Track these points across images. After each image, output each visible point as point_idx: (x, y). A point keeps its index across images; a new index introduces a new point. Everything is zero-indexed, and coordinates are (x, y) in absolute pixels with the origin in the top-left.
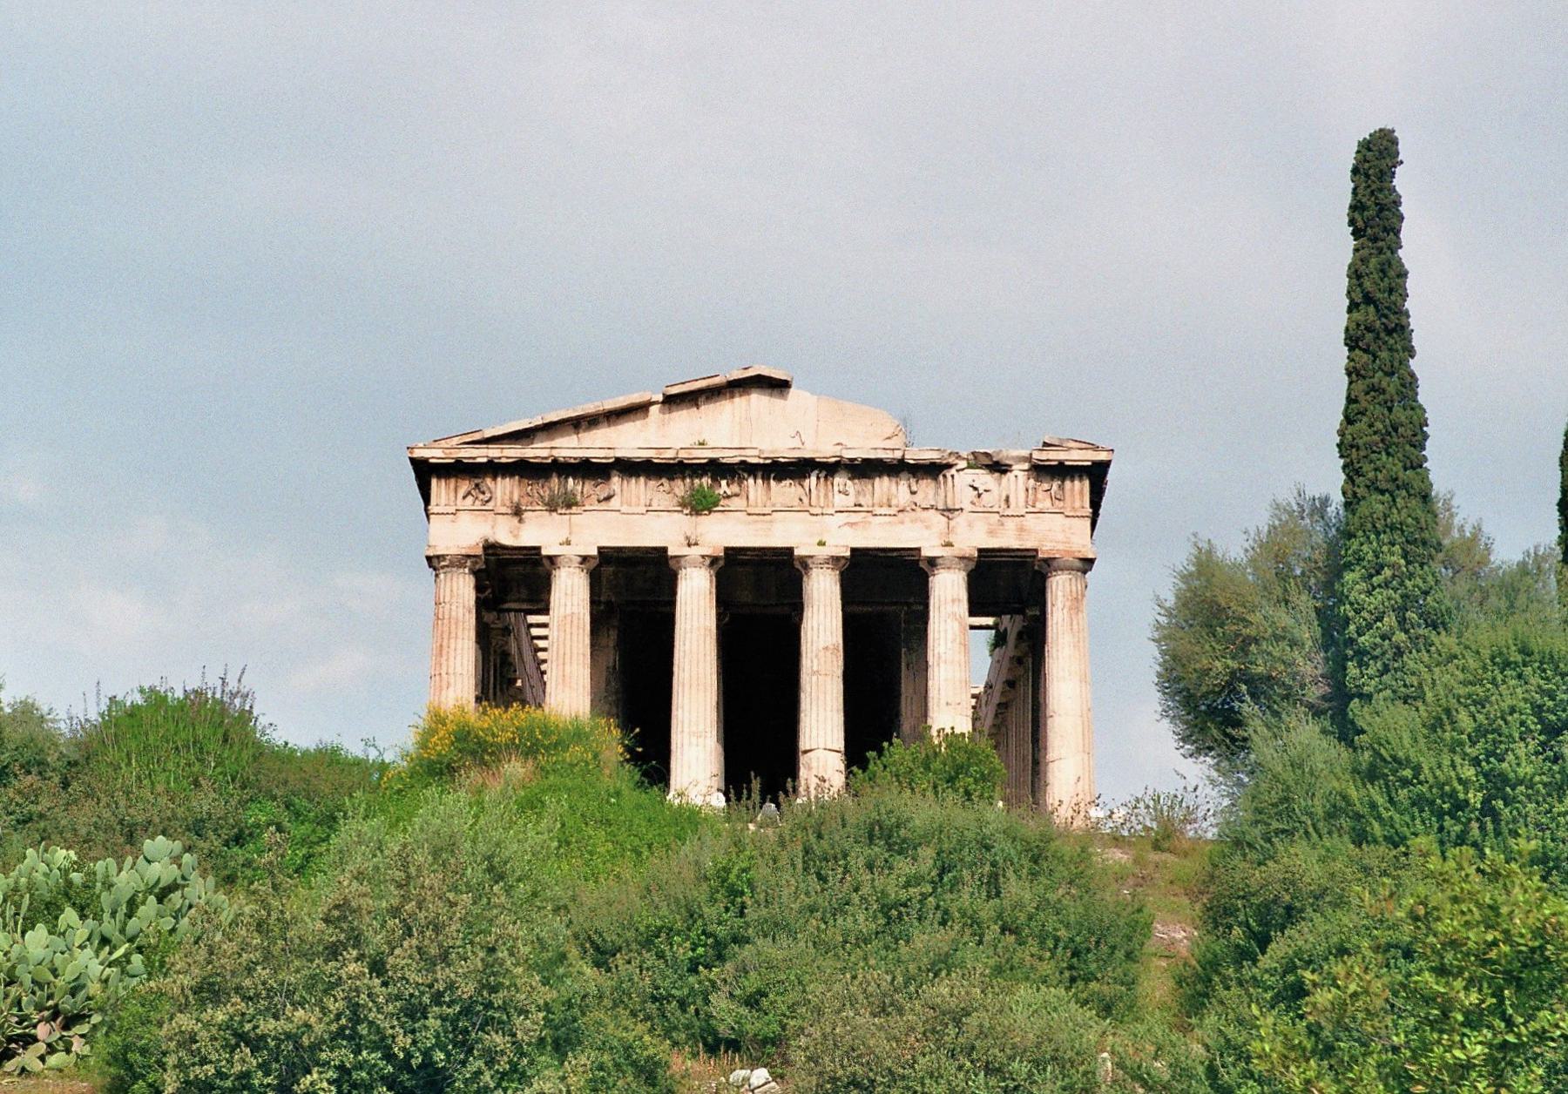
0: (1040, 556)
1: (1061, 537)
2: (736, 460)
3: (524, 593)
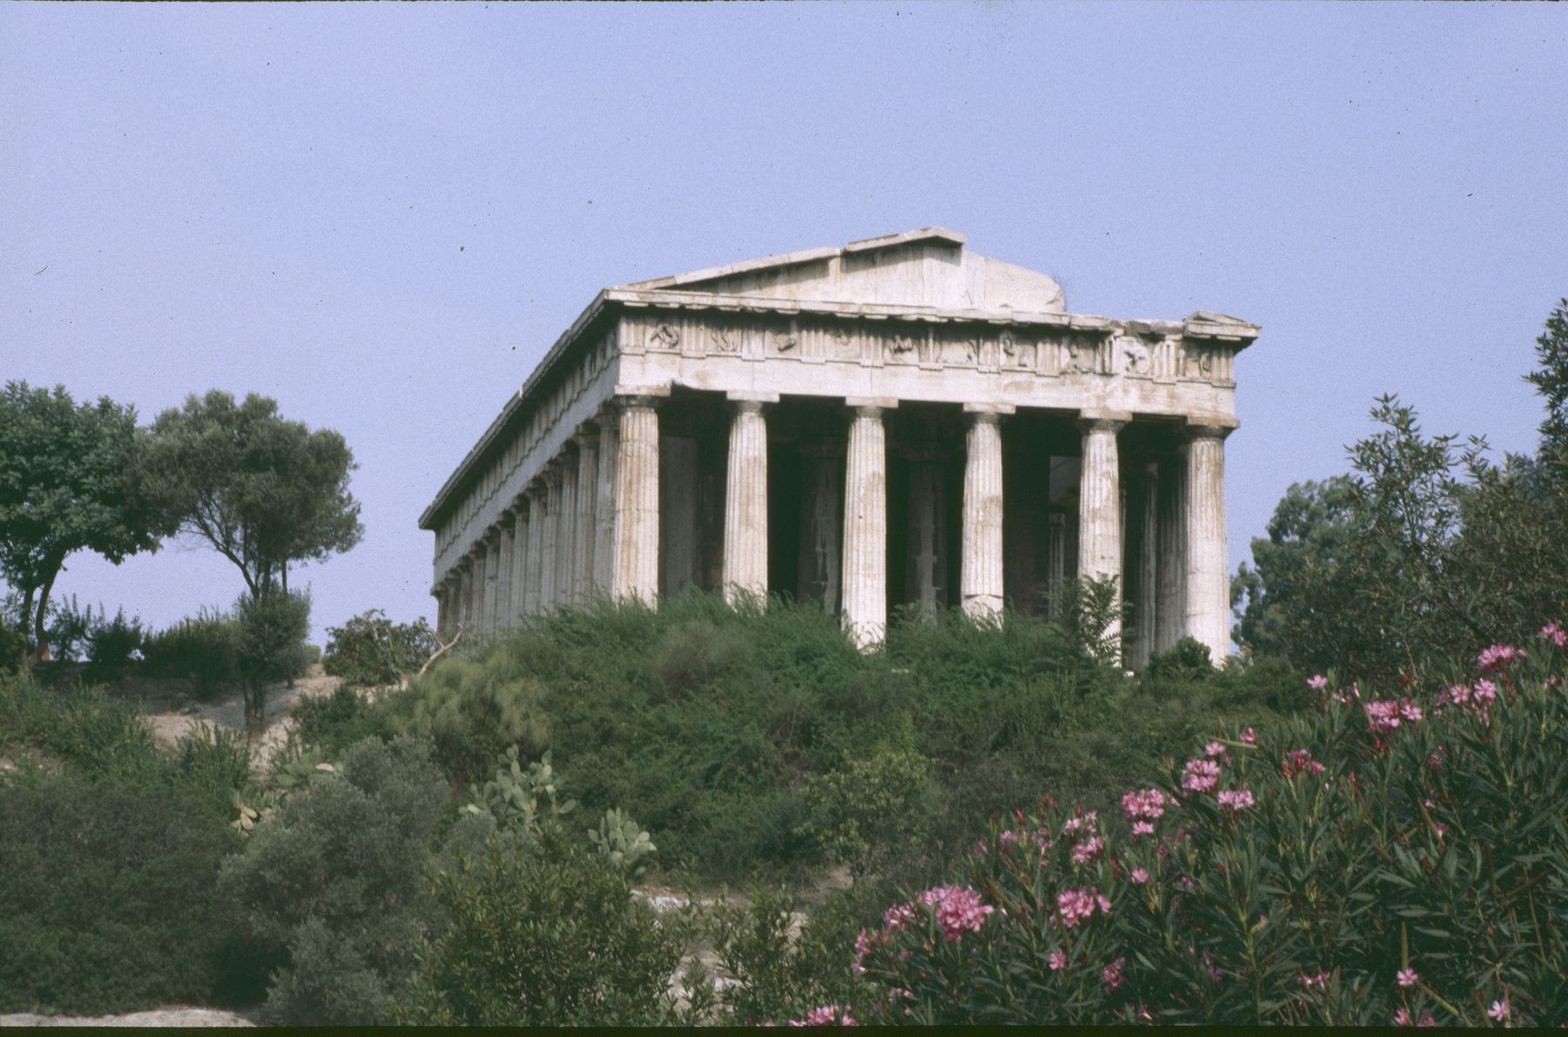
1: (1208, 405)
2: (914, 318)
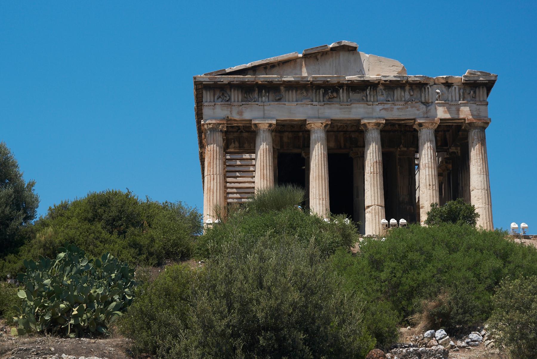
0: (466, 122)
2: (336, 82)
3: (237, 144)
